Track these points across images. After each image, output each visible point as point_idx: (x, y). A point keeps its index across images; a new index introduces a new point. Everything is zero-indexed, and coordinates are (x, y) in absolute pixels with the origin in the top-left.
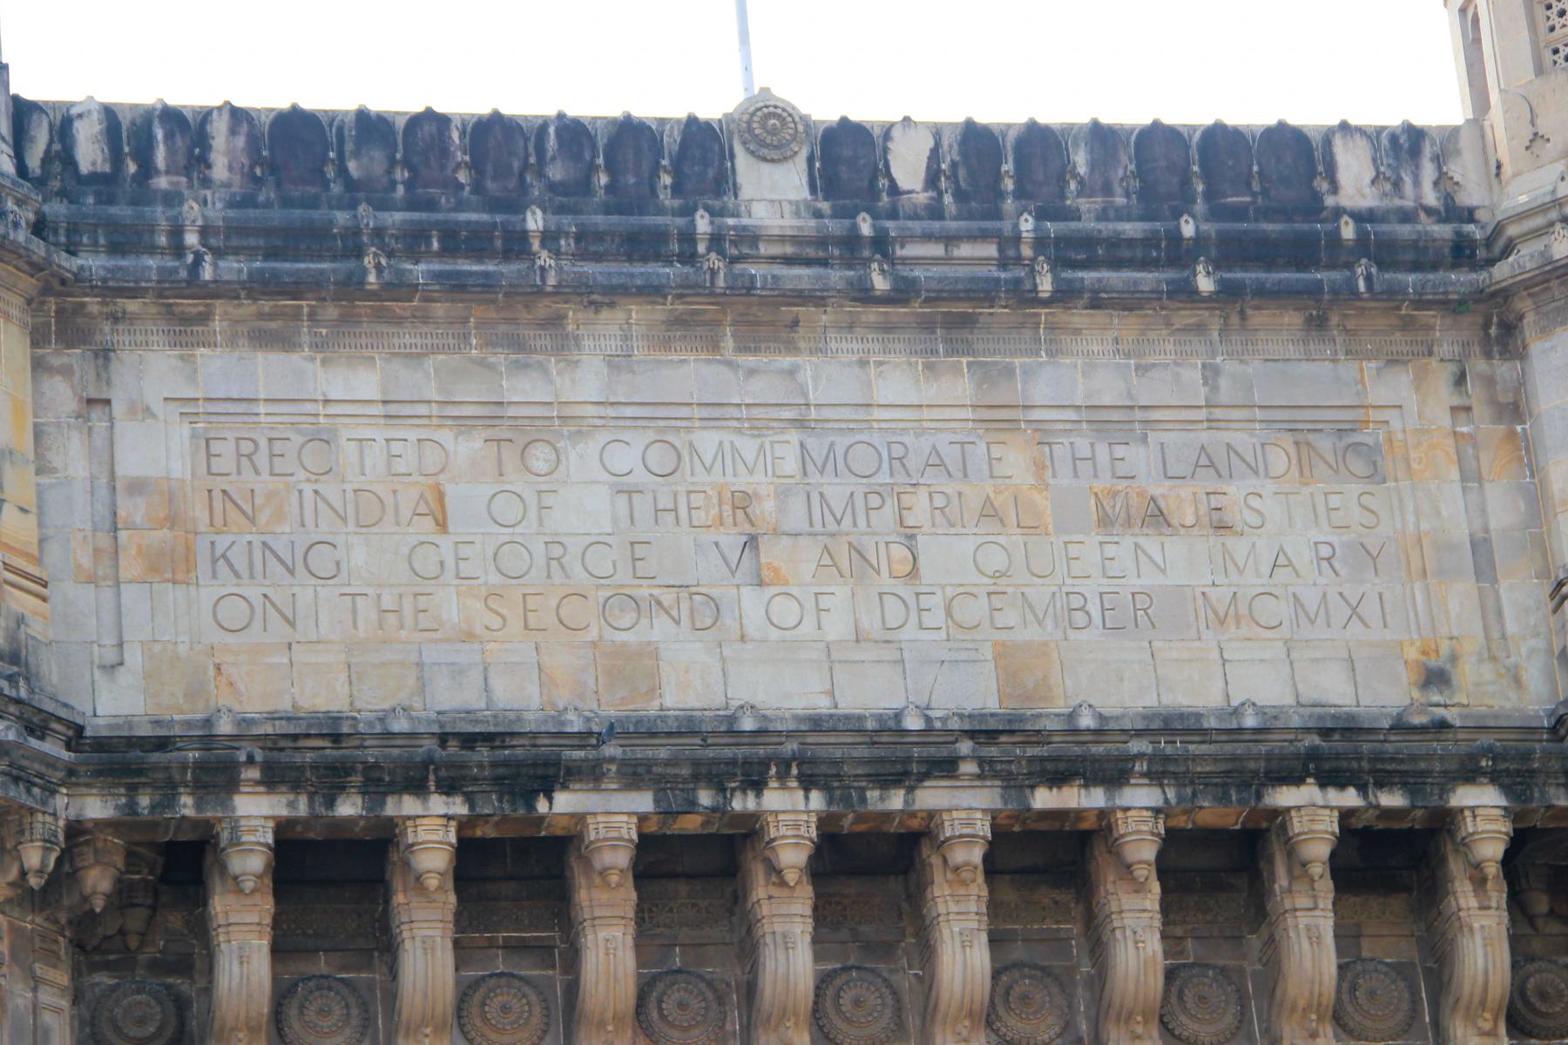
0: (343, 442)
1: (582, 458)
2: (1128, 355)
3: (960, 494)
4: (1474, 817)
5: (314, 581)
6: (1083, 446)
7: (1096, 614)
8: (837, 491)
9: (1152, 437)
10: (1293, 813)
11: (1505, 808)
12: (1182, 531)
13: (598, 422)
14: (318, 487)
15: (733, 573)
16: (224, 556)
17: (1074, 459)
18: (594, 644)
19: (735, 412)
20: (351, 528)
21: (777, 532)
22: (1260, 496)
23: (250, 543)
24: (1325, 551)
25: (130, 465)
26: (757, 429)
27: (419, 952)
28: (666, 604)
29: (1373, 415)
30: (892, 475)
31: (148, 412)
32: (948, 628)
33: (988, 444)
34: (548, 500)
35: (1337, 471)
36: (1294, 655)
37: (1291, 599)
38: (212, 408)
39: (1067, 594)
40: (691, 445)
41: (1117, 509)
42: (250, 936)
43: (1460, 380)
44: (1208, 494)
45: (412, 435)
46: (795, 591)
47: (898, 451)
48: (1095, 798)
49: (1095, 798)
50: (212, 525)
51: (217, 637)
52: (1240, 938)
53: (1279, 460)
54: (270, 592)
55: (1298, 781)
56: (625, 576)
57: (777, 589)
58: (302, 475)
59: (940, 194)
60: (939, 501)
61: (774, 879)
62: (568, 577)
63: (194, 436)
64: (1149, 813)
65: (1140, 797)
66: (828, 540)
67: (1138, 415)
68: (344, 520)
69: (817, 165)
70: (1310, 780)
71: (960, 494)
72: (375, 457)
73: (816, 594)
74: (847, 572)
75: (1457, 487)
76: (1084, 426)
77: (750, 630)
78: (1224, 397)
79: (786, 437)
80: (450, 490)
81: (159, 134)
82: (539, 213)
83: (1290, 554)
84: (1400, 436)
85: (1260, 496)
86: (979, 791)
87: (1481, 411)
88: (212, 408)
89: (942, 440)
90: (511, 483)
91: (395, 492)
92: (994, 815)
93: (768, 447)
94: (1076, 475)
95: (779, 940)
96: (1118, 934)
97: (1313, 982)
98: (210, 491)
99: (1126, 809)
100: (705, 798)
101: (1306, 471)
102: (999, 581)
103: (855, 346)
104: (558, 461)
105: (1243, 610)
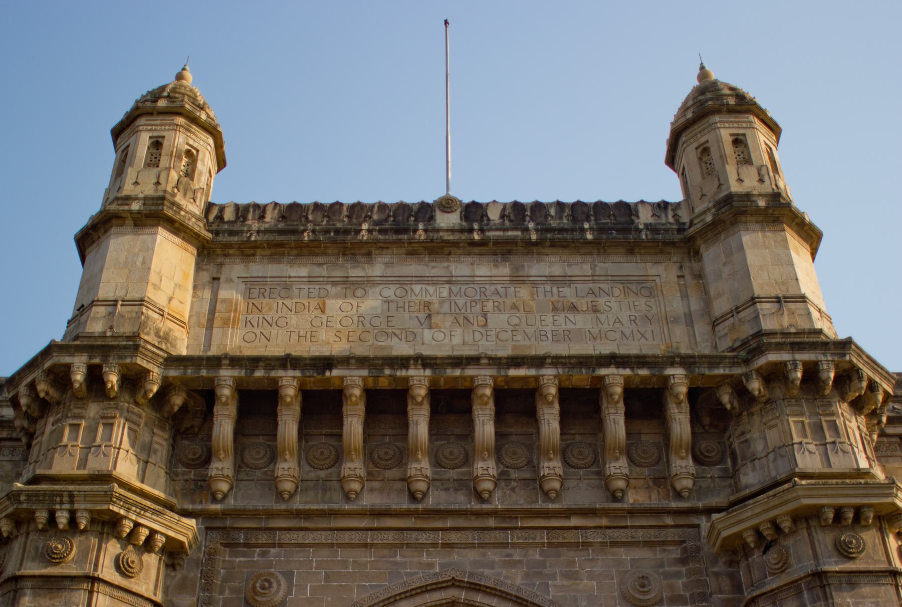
2: (564, 262)
3: (504, 302)
4: (674, 378)
5: (278, 328)
6: (548, 288)
7: (550, 336)
8: (461, 302)
9: (572, 285)
10: (606, 377)
11: (686, 375)
13: (380, 282)
14: (284, 302)
16: (250, 321)
17: (545, 292)
18: (370, 346)
19: (427, 279)
21: (438, 313)
24: (633, 318)
26: (434, 283)
27: (283, 425)
28: (397, 334)
29: (650, 278)
30: (480, 297)
31: (231, 281)
33: (515, 288)
35: (637, 295)
36: (620, 348)
37: (620, 333)
38: (252, 280)
40: (411, 289)
43: (681, 267)
45: (317, 287)
46: (443, 330)
47: (483, 290)
48: (532, 372)
49: (532, 372)
51: (243, 344)
52: (596, 434)
53: (617, 292)
54: (263, 331)
55: (608, 365)
56: (384, 326)
57: (437, 330)
59: (504, 220)
60: (496, 304)
61: (414, 402)
63: (246, 288)
64: (552, 377)
65: (548, 371)
66: (456, 316)
68: (291, 311)
69: (463, 213)
70: (612, 366)
71: (504, 302)
74: (462, 325)
75: (680, 298)
76: (549, 282)
77: (426, 341)
78: (597, 273)
79: (445, 286)
81: (251, 210)
82: (367, 225)
83: (620, 318)
87: (688, 277)
88: (252, 280)
89: (499, 287)
91: (309, 303)
92: (494, 378)
93: (438, 289)
94: (545, 296)
95: (415, 422)
96: (542, 422)
97: (616, 438)
99: (543, 376)
100: (387, 372)
101: (627, 294)
103: (470, 259)
105: (603, 335)
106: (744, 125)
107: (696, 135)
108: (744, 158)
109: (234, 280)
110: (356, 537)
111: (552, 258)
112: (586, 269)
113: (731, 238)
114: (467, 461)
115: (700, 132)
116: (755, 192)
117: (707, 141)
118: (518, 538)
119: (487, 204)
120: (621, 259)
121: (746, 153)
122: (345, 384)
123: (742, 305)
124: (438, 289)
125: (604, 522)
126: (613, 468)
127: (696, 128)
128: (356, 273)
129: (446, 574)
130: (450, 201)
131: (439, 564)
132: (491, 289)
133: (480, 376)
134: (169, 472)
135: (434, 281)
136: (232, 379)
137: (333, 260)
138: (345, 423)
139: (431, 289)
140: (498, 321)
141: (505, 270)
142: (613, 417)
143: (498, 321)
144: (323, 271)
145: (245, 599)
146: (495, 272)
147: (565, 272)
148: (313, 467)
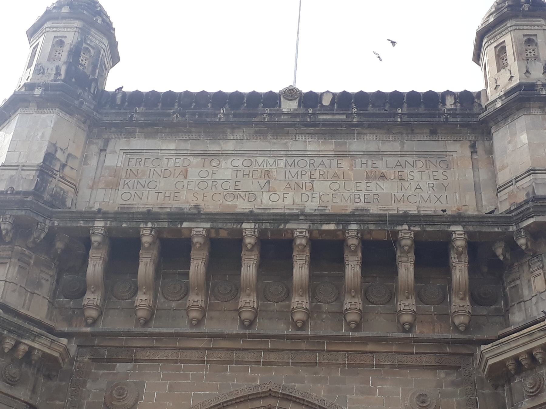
0: (164, 159)
1: (226, 164)
6: (364, 161)
7: (362, 199)
8: (294, 171)
12: (390, 180)
15: (262, 189)
18: (220, 204)
20: (162, 178)
22: (414, 172)
23: (134, 181)
24: (432, 185)
25: (108, 163)
28: (242, 196)
29: (448, 153)
30: (310, 167)
31: (115, 152)
32: (319, 202)
34: (214, 172)
37: (420, 196)
38: (131, 151)
39: (355, 194)
40: (256, 160)
41: (372, 175)
42: (97, 260)
44: (399, 172)
50: (126, 177)
56: (232, 189)
58: (152, 166)
60: (322, 173)
62: (216, 189)
65: (354, 227)
67: (381, 153)
68: (160, 176)
71: (328, 171)
72: (171, 163)
73: (284, 194)
76: (365, 156)
80: (189, 169)
83: (420, 186)
84: (456, 158)
85: (414, 172)
86: (305, 224)
88: (131, 151)
89: (325, 160)
90: (206, 168)
92: (310, 231)
93: (277, 161)
94: (361, 167)
96: (347, 266)
98: (127, 170)
102: (336, 191)
104: (220, 163)
106: (536, 27)
107: (496, 36)
108: (534, 55)
109: (117, 151)
110: (195, 355)
111: (368, 137)
112: (397, 146)
113: (516, 120)
114: (288, 296)
115: (499, 34)
116: (539, 83)
117: (504, 41)
118: (324, 359)
119: (322, 94)
120: (426, 138)
121: (536, 50)
122: (192, 234)
123: (520, 176)
124: (277, 161)
125: (394, 349)
126: (403, 305)
127: (497, 30)
128: (213, 147)
129: (265, 387)
130: (292, 91)
131: (260, 378)
132: (318, 161)
133: (298, 229)
134: (51, 301)
135: (274, 155)
136: (103, 228)
137: (196, 137)
138: (192, 264)
139: (271, 161)
140: (321, 186)
141: (331, 146)
142: (404, 264)
143: (321, 186)
144: (188, 146)
145: (105, 403)
146: (323, 148)
147: (378, 149)
148: (167, 299)
